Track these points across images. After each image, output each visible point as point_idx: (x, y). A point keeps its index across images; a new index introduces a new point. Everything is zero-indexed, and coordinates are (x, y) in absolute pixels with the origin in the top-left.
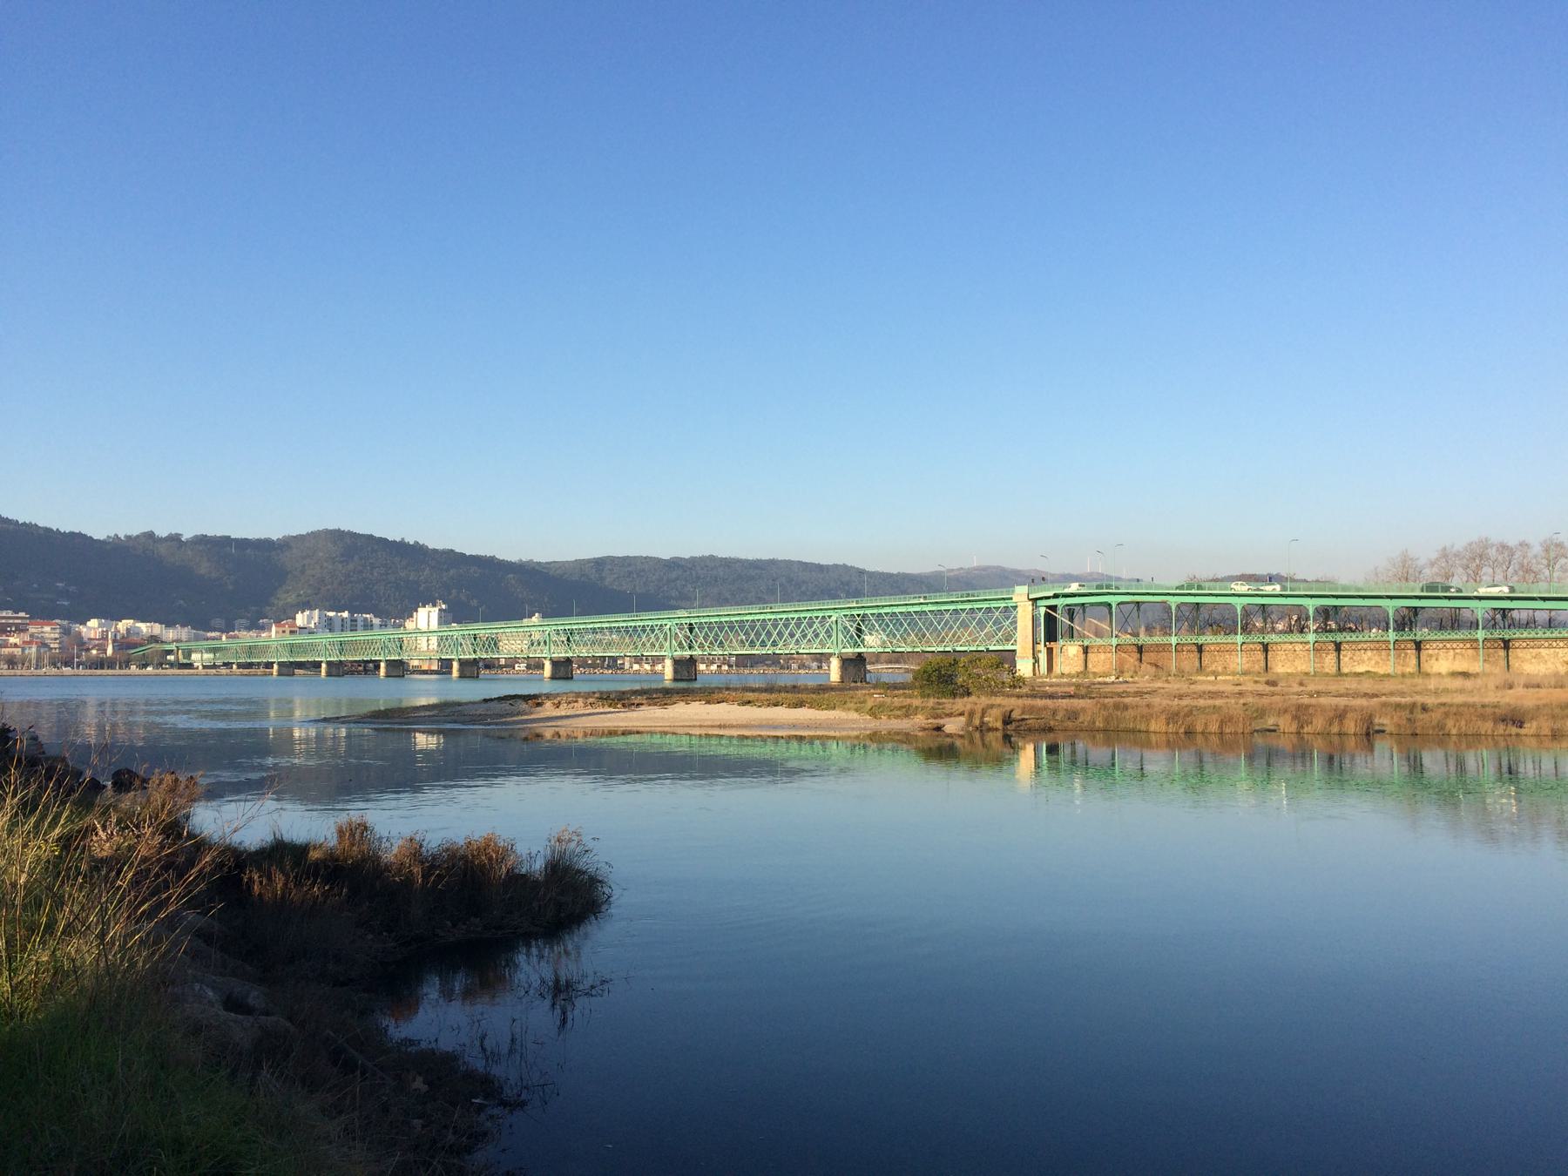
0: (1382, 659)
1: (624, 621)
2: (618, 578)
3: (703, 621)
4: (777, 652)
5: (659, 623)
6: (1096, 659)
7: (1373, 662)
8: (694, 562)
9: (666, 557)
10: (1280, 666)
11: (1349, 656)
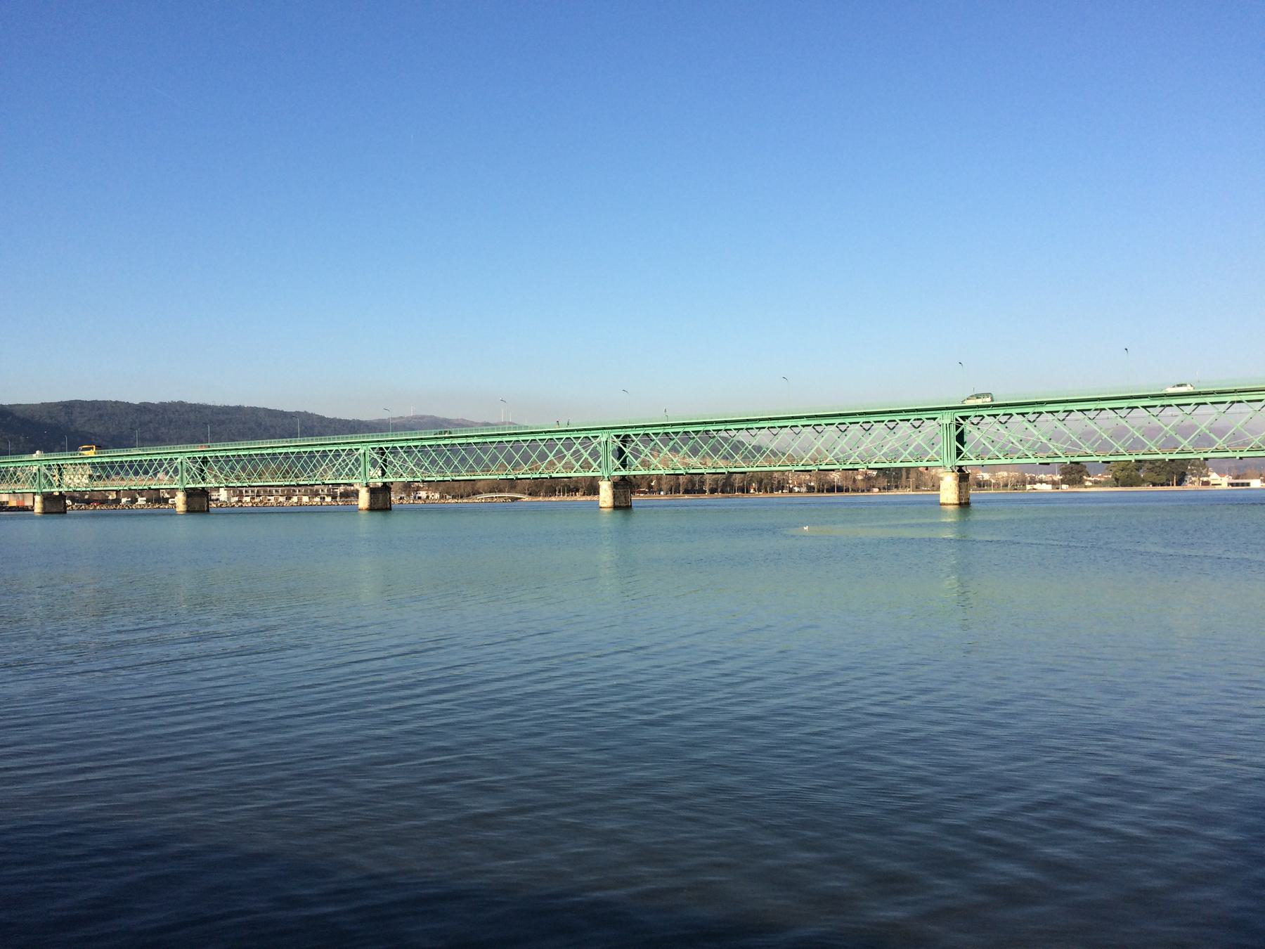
2: (89, 420)
4: (554, 475)
5: (169, 458)
8: (164, 407)
9: (136, 400)
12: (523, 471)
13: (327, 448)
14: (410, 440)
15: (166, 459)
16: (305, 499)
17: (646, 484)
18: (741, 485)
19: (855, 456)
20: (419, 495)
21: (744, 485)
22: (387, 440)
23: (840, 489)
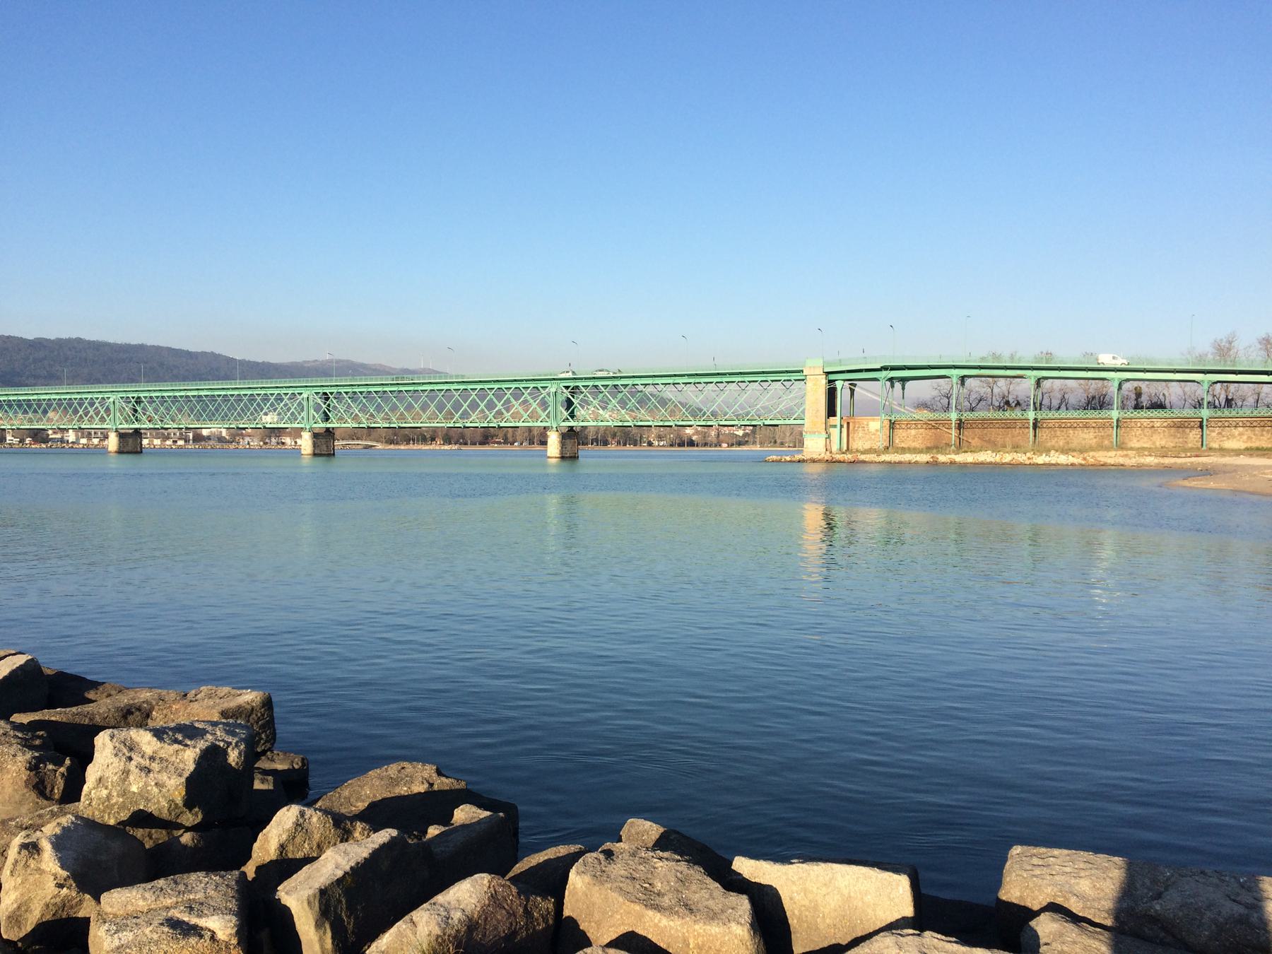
0: (1254, 435)
1: (261, 388)
3: (357, 390)
4: (502, 424)
6: (904, 435)
7: (1245, 437)
10: (1135, 441)
11: (1217, 432)
12: (471, 419)
13: (269, 392)
14: (355, 385)
15: (97, 398)
16: (157, 442)
17: (501, 435)
18: (595, 437)
19: (753, 413)
20: (283, 441)
21: (597, 437)
22: (330, 384)
23: (691, 443)
